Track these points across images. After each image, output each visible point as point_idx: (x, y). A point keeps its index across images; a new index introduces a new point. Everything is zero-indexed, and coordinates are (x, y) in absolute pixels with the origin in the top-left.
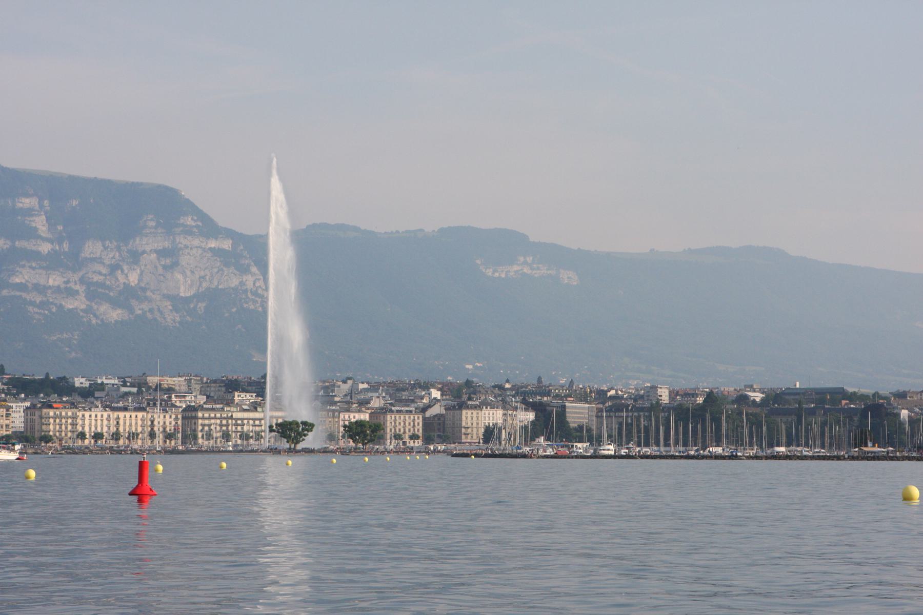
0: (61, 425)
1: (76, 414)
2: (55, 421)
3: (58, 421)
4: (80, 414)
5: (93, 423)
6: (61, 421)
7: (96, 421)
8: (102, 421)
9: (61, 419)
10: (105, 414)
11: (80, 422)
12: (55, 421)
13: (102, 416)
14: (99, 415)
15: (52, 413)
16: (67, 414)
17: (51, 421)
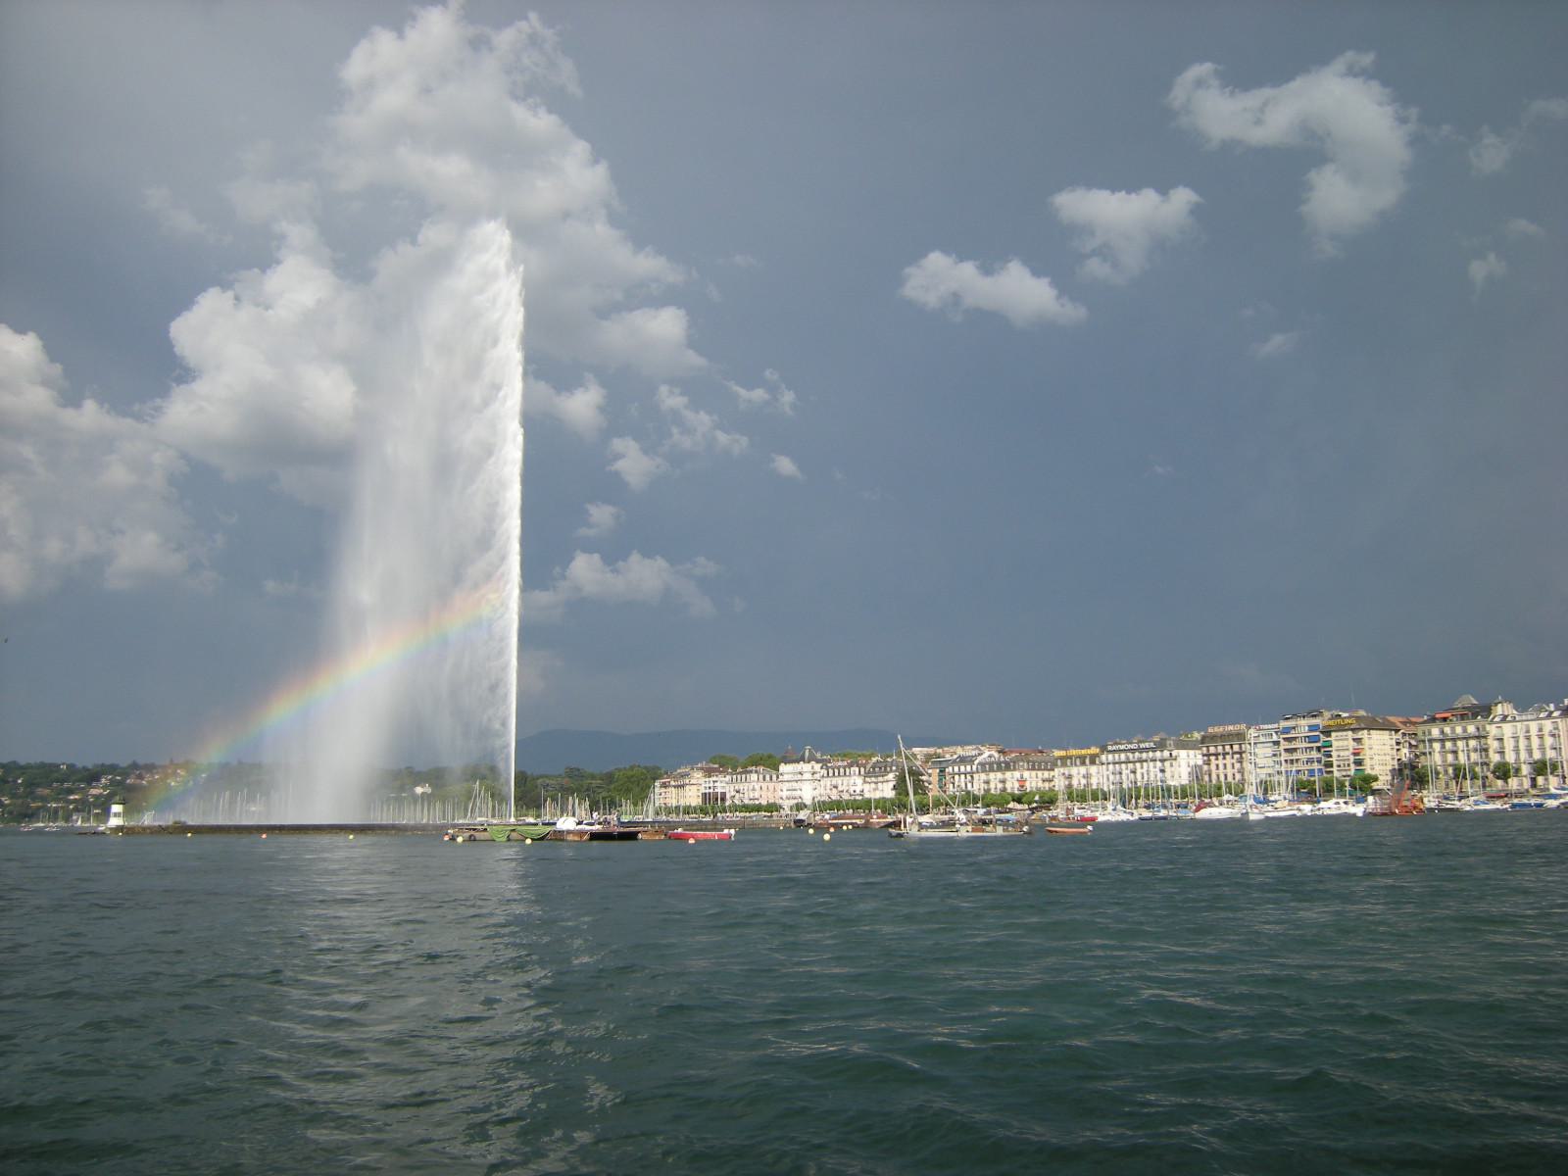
0: (1455, 752)
1: (1484, 729)
2: (1443, 747)
3: (1449, 745)
4: (1492, 730)
5: (1522, 744)
6: (1455, 745)
7: (1528, 738)
8: (1541, 737)
9: (1454, 740)
10: (1548, 725)
11: (1494, 745)
12: (1443, 747)
13: (1540, 730)
14: (1534, 726)
15: (1435, 732)
16: (1465, 730)
17: (1437, 746)
